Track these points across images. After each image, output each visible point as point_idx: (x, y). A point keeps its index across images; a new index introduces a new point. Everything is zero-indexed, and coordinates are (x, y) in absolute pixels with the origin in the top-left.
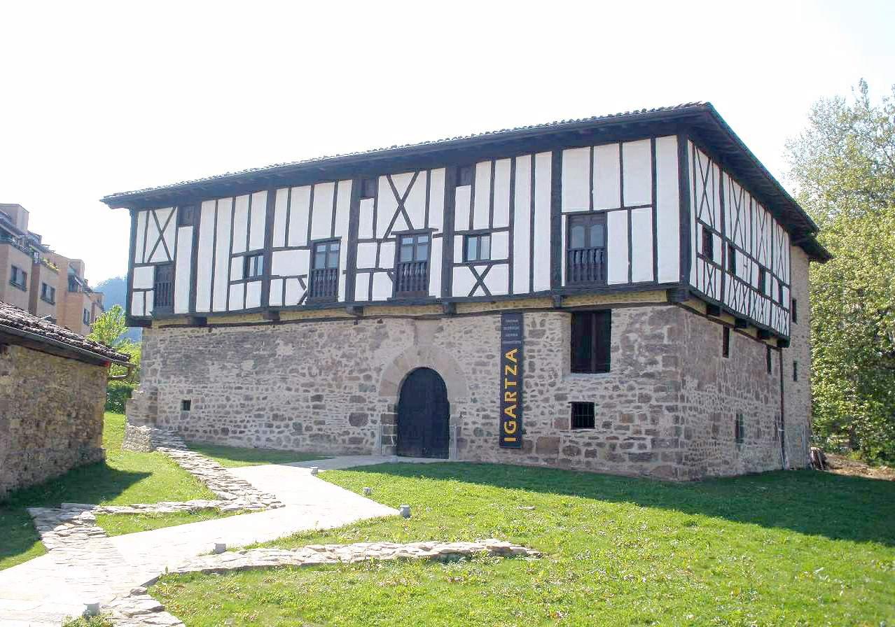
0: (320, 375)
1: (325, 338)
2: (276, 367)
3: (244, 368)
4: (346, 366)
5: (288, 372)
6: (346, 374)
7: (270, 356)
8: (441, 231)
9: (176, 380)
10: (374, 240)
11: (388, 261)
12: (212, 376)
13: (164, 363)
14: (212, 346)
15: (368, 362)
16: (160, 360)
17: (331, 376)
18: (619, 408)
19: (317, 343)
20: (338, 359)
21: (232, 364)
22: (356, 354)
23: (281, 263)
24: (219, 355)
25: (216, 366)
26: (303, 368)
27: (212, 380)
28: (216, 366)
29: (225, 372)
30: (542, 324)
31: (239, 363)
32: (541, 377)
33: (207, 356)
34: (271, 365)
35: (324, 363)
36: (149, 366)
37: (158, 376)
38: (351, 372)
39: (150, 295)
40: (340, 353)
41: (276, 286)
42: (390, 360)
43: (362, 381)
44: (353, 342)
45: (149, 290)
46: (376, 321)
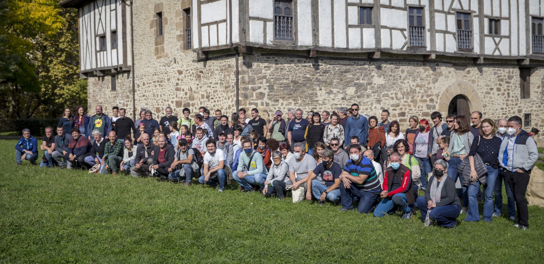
0: (403, 98)
1: (406, 73)
2: (373, 92)
3: (348, 92)
4: (419, 92)
5: (381, 96)
6: (419, 98)
7: (370, 84)
8: (477, 13)
9: (285, 103)
10: (443, 12)
11: (452, 27)
12: (320, 99)
13: (271, 88)
14: (319, 74)
15: (432, 90)
16: (265, 84)
17: (410, 99)
18: (540, 116)
19: (401, 77)
20: (414, 88)
21: (338, 90)
22: (425, 85)
23: (386, 17)
24: (326, 82)
25: (323, 92)
26: (392, 94)
27: (320, 102)
28: (323, 92)
29: (332, 96)
30: (513, 73)
31: (343, 89)
32: (512, 101)
33: (315, 83)
34: (369, 91)
35: (405, 90)
36: (254, 89)
37: (266, 99)
38: (422, 97)
39: (270, 26)
40: (415, 84)
41: (384, 33)
42: (444, 89)
43: (428, 103)
44: (423, 77)
45: (270, 20)
46: (435, 64)
